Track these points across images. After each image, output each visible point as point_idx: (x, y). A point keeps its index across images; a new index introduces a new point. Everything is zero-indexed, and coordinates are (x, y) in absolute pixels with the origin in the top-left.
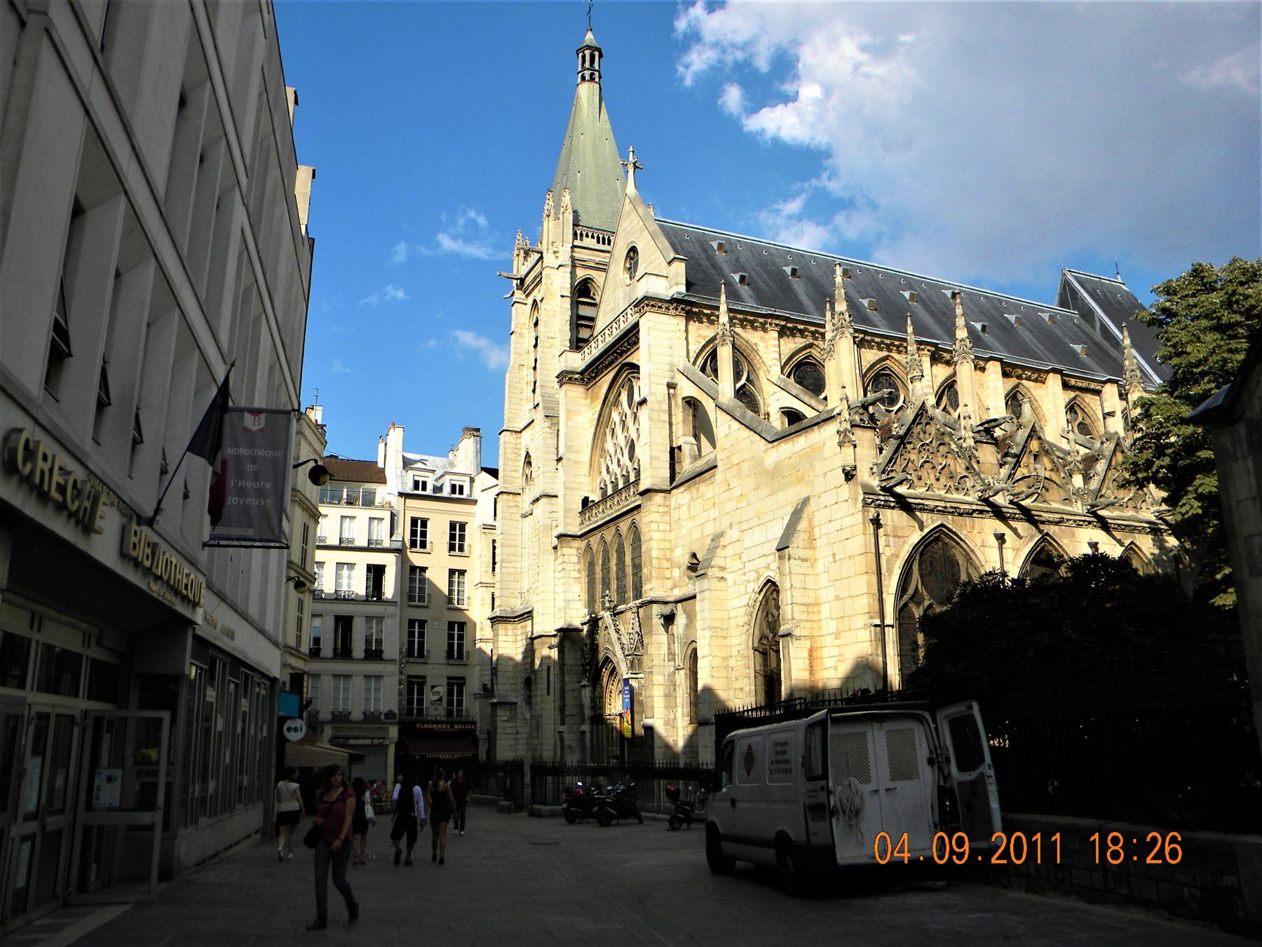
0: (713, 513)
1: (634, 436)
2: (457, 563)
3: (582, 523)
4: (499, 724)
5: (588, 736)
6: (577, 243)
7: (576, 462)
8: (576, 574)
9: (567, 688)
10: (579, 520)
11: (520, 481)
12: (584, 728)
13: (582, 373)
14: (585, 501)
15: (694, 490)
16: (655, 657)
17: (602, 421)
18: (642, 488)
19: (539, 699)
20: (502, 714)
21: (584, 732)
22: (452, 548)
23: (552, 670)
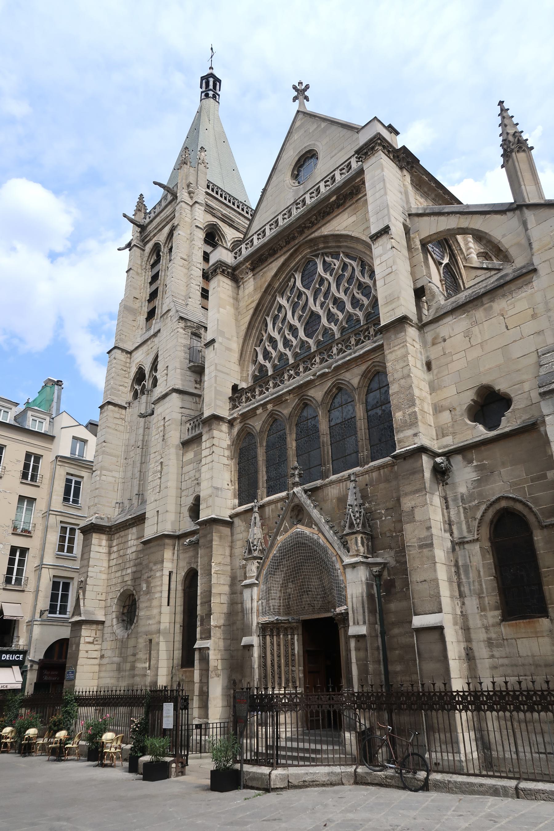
0: (530, 327)
1: (317, 309)
2: (28, 491)
3: (234, 407)
4: (82, 647)
5: (256, 652)
6: (210, 191)
7: (229, 349)
8: (226, 462)
9: (214, 591)
10: (228, 406)
11: (129, 397)
12: (245, 641)
13: (235, 269)
14: (235, 388)
15: (479, 314)
16: (433, 523)
17: (262, 310)
18: (383, 323)
19: (155, 611)
20: (87, 633)
21: (250, 647)
22: (25, 476)
23: (174, 576)
